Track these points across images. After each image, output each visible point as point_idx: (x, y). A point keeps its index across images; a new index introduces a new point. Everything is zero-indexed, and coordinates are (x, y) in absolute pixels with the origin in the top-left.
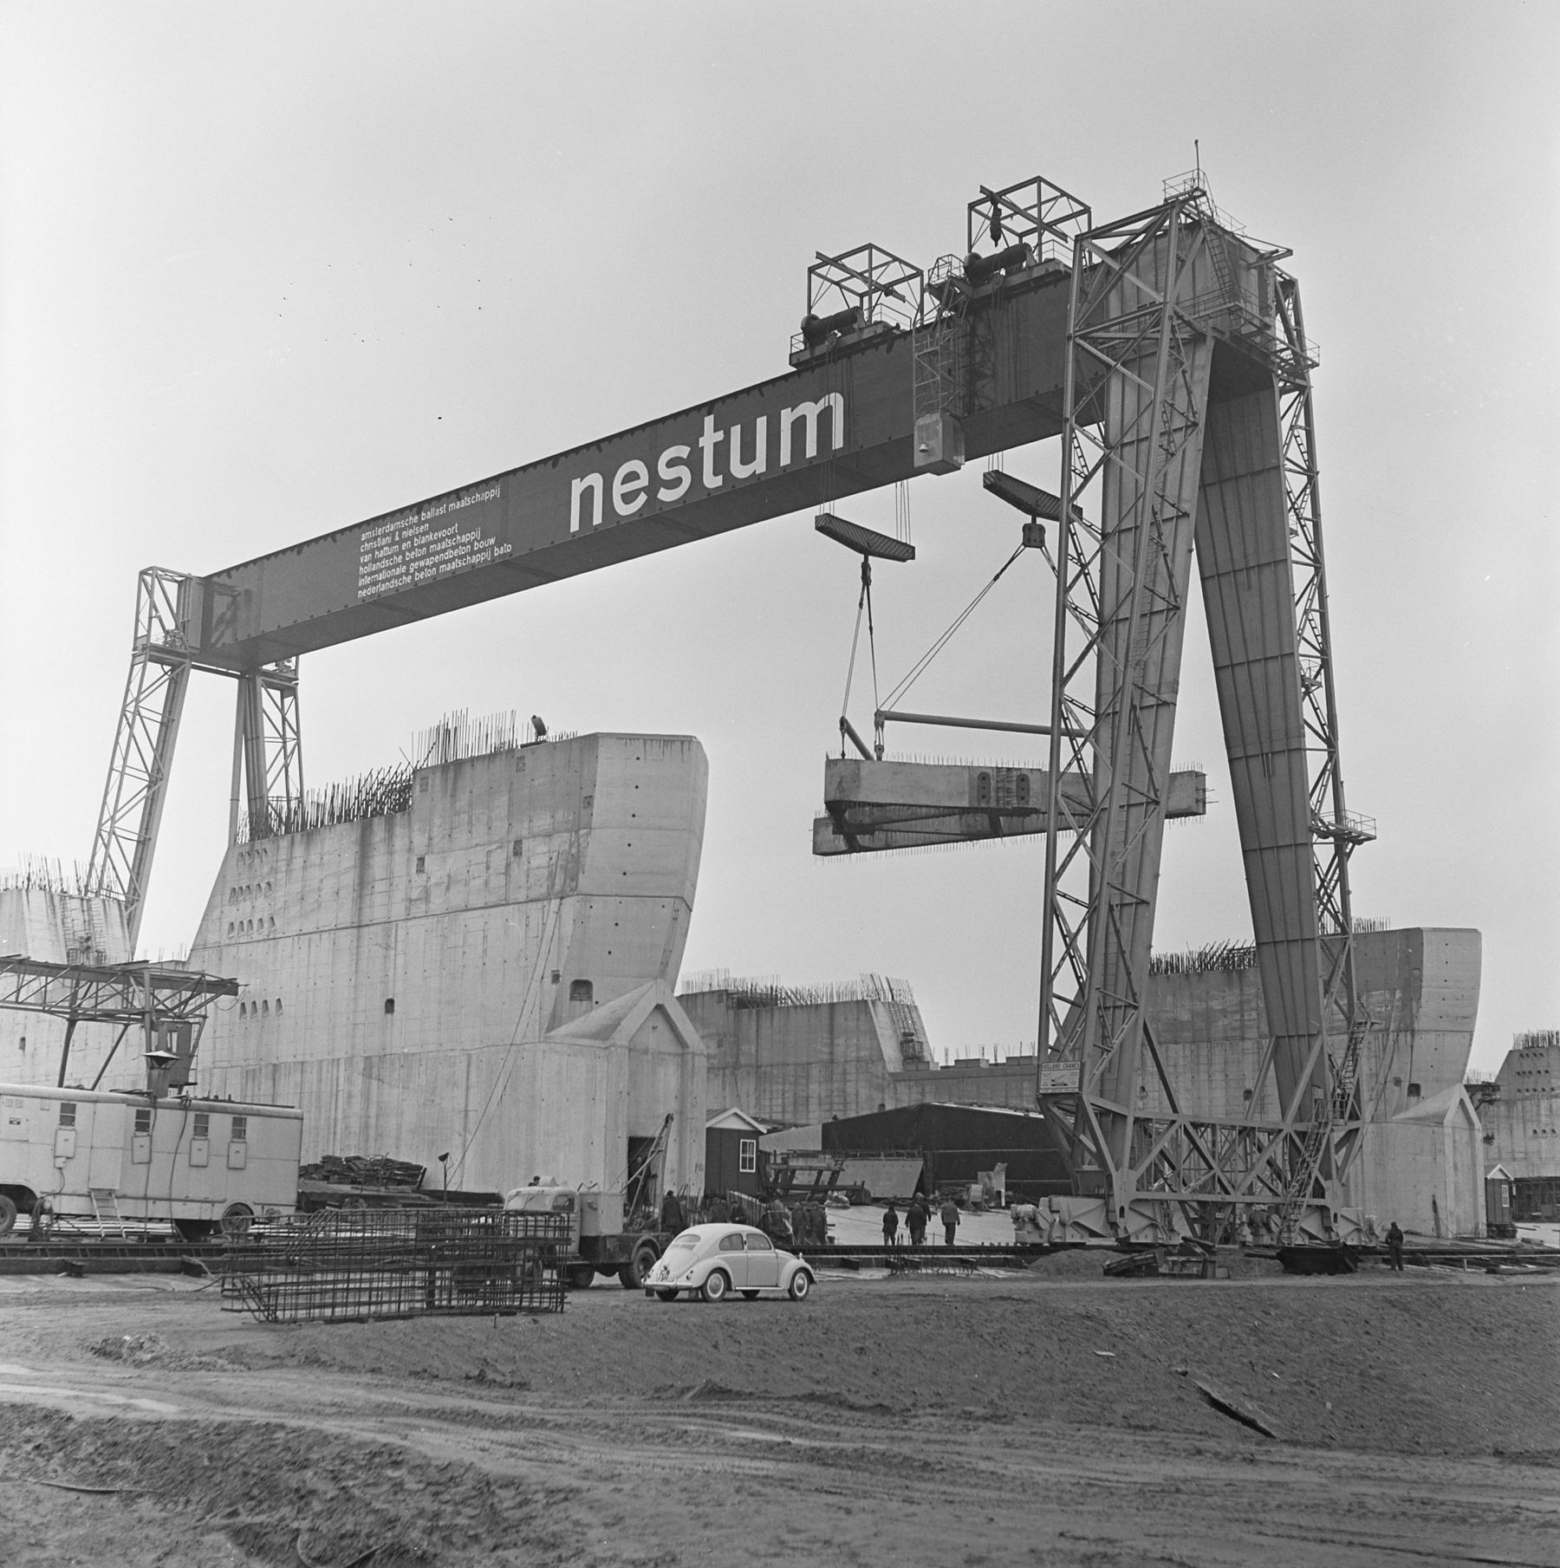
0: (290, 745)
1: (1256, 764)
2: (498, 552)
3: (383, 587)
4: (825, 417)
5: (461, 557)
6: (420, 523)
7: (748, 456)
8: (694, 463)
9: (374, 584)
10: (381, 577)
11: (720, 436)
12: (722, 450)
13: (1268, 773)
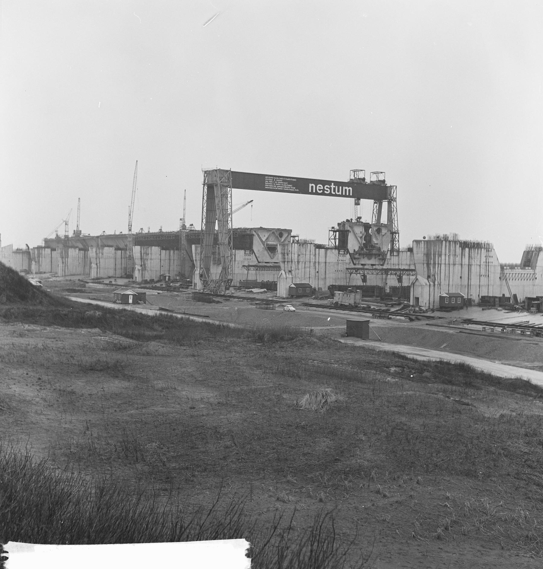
4: (349, 190)
7: (338, 191)
8: (330, 189)
11: (334, 187)
12: (334, 189)
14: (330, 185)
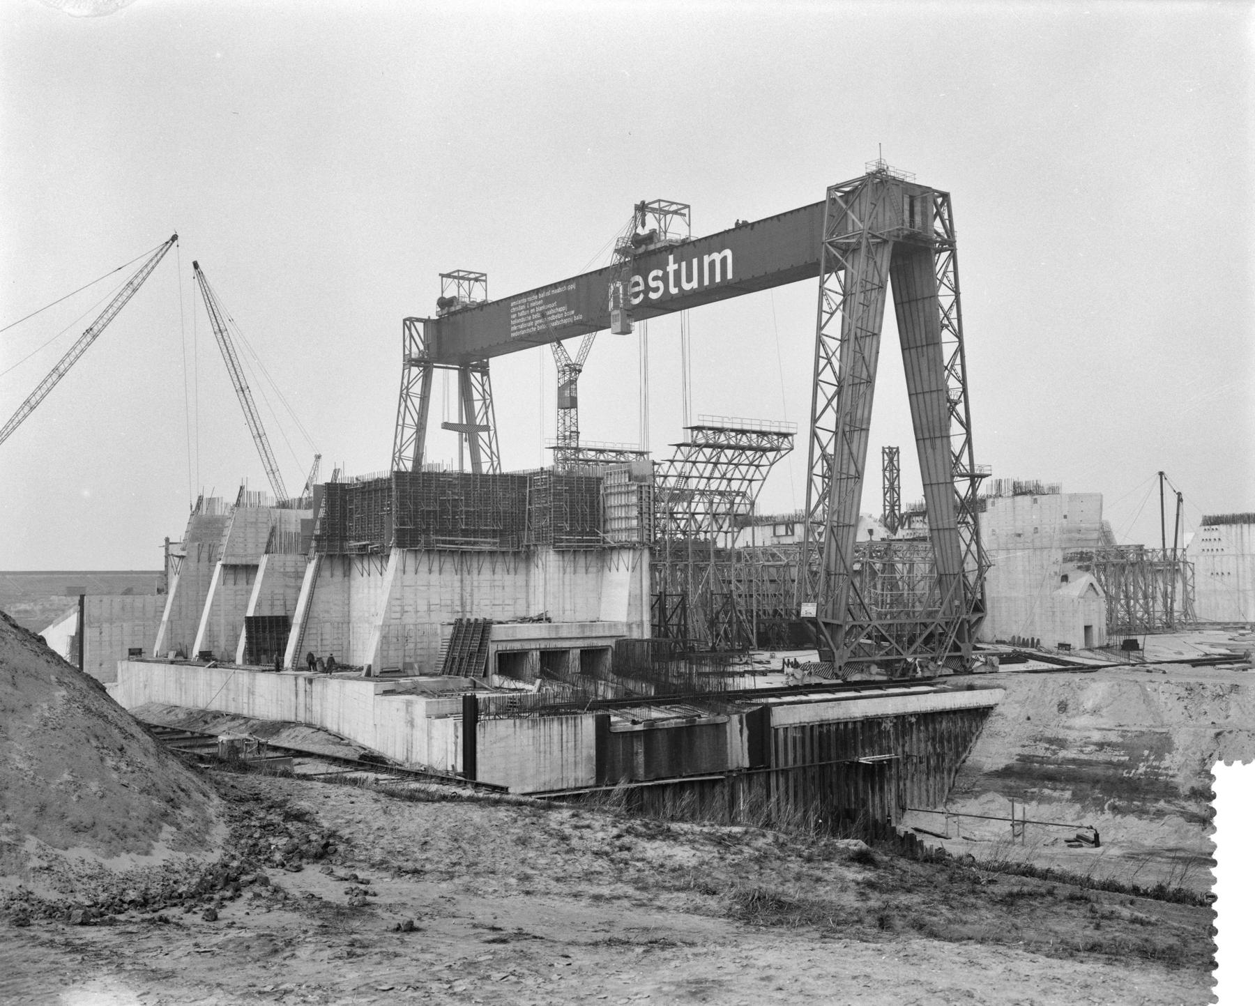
0: (488, 402)
1: (928, 443)
2: (576, 318)
3: (523, 332)
4: (724, 260)
5: (559, 319)
6: (538, 300)
7: (689, 280)
8: (665, 279)
9: (519, 330)
10: (521, 327)
11: (676, 266)
12: (677, 273)
13: (934, 448)
14: (663, 265)
